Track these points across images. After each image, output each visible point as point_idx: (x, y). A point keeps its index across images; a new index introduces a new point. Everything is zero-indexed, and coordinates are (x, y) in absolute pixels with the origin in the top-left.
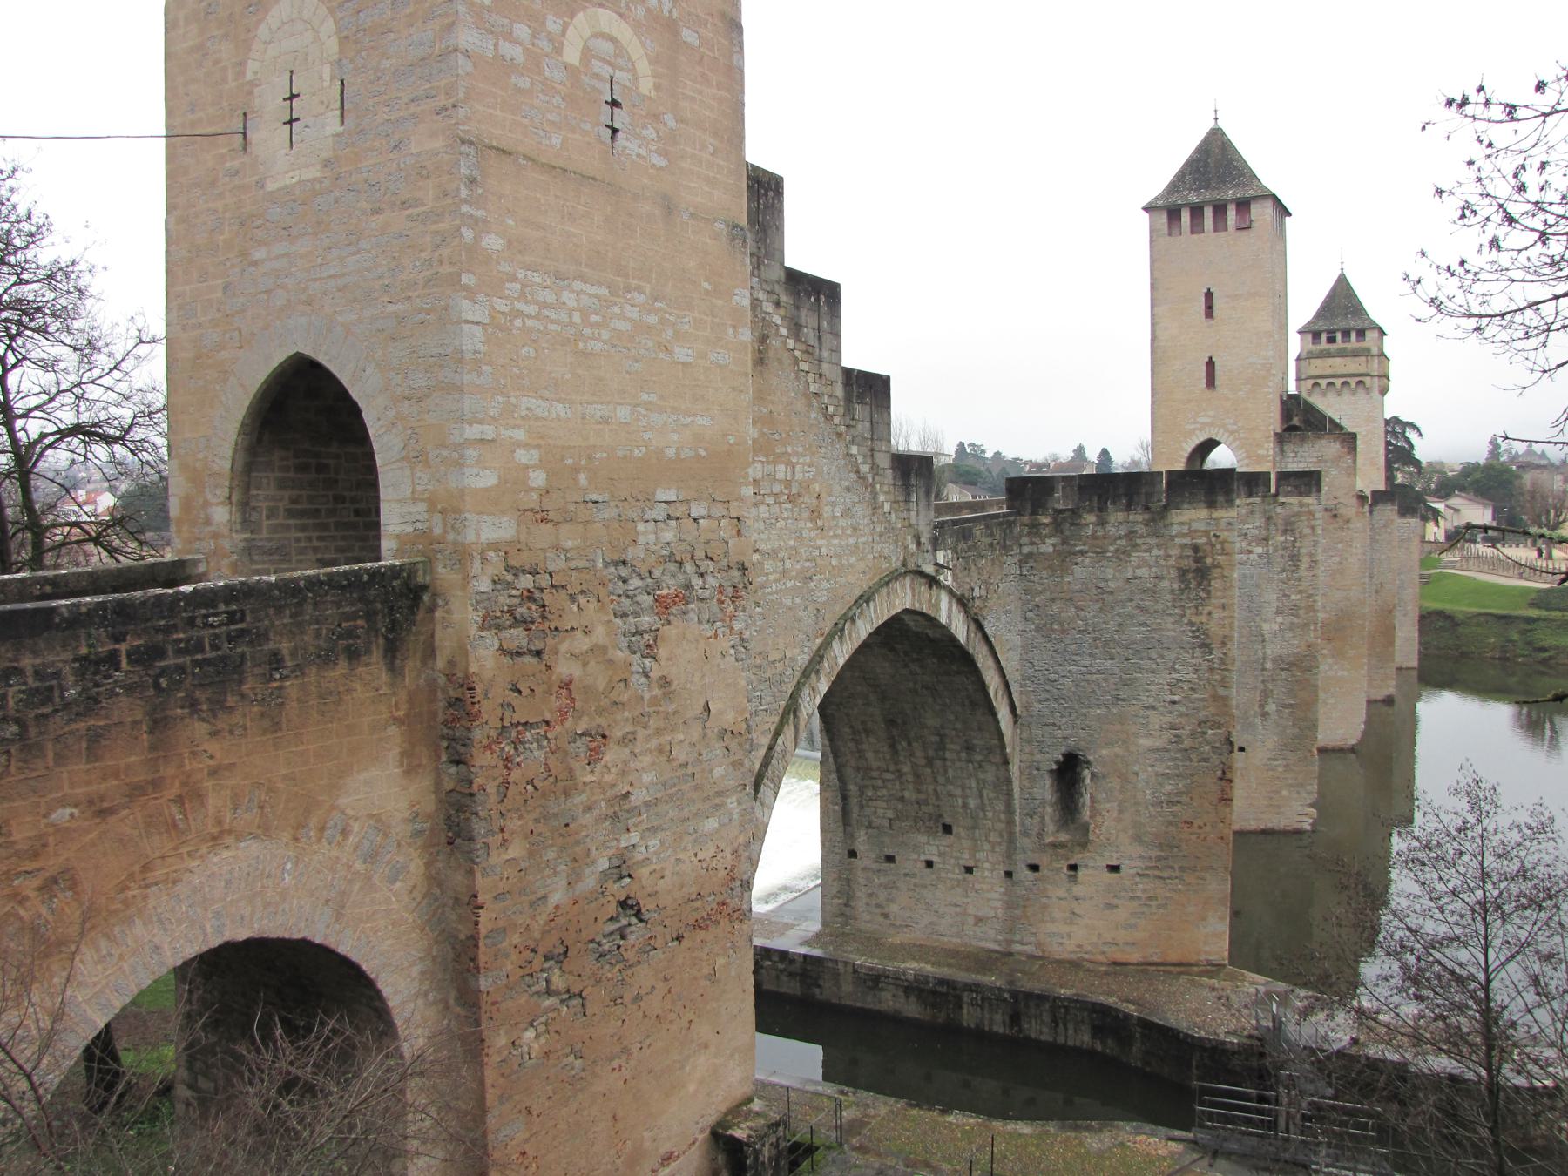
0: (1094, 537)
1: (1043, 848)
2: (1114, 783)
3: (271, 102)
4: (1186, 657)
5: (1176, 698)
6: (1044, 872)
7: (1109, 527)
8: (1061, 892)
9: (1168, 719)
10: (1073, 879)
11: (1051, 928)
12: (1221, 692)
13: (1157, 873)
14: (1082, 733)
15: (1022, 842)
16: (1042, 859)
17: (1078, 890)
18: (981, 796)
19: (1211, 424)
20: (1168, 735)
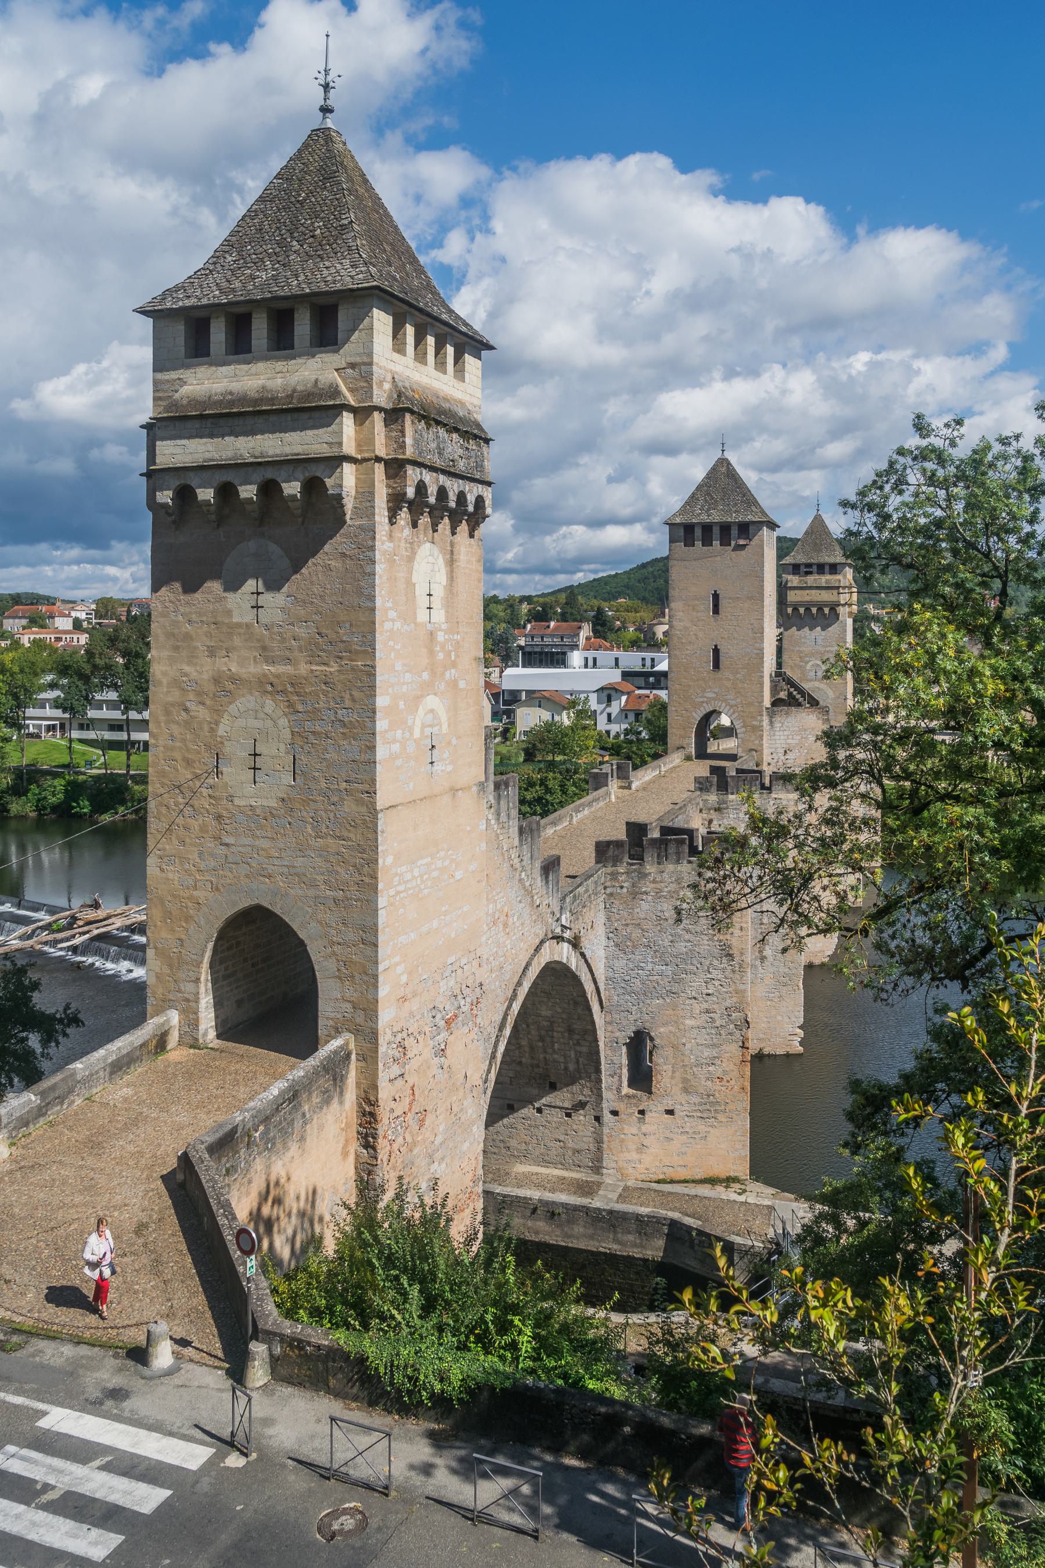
1: (621, 1098)
2: (669, 1052)
4: (716, 962)
6: (622, 1116)
7: (665, 875)
8: (634, 1131)
9: (705, 1006)
10: (642, 1121)
11: (627, 1156)
12: (742, 987)
14: (647, 1017)
15: (606, 1094)
16: (620, 1107)
17: (644, 1128)
18: (578, 1062)
20: (705, 1017)
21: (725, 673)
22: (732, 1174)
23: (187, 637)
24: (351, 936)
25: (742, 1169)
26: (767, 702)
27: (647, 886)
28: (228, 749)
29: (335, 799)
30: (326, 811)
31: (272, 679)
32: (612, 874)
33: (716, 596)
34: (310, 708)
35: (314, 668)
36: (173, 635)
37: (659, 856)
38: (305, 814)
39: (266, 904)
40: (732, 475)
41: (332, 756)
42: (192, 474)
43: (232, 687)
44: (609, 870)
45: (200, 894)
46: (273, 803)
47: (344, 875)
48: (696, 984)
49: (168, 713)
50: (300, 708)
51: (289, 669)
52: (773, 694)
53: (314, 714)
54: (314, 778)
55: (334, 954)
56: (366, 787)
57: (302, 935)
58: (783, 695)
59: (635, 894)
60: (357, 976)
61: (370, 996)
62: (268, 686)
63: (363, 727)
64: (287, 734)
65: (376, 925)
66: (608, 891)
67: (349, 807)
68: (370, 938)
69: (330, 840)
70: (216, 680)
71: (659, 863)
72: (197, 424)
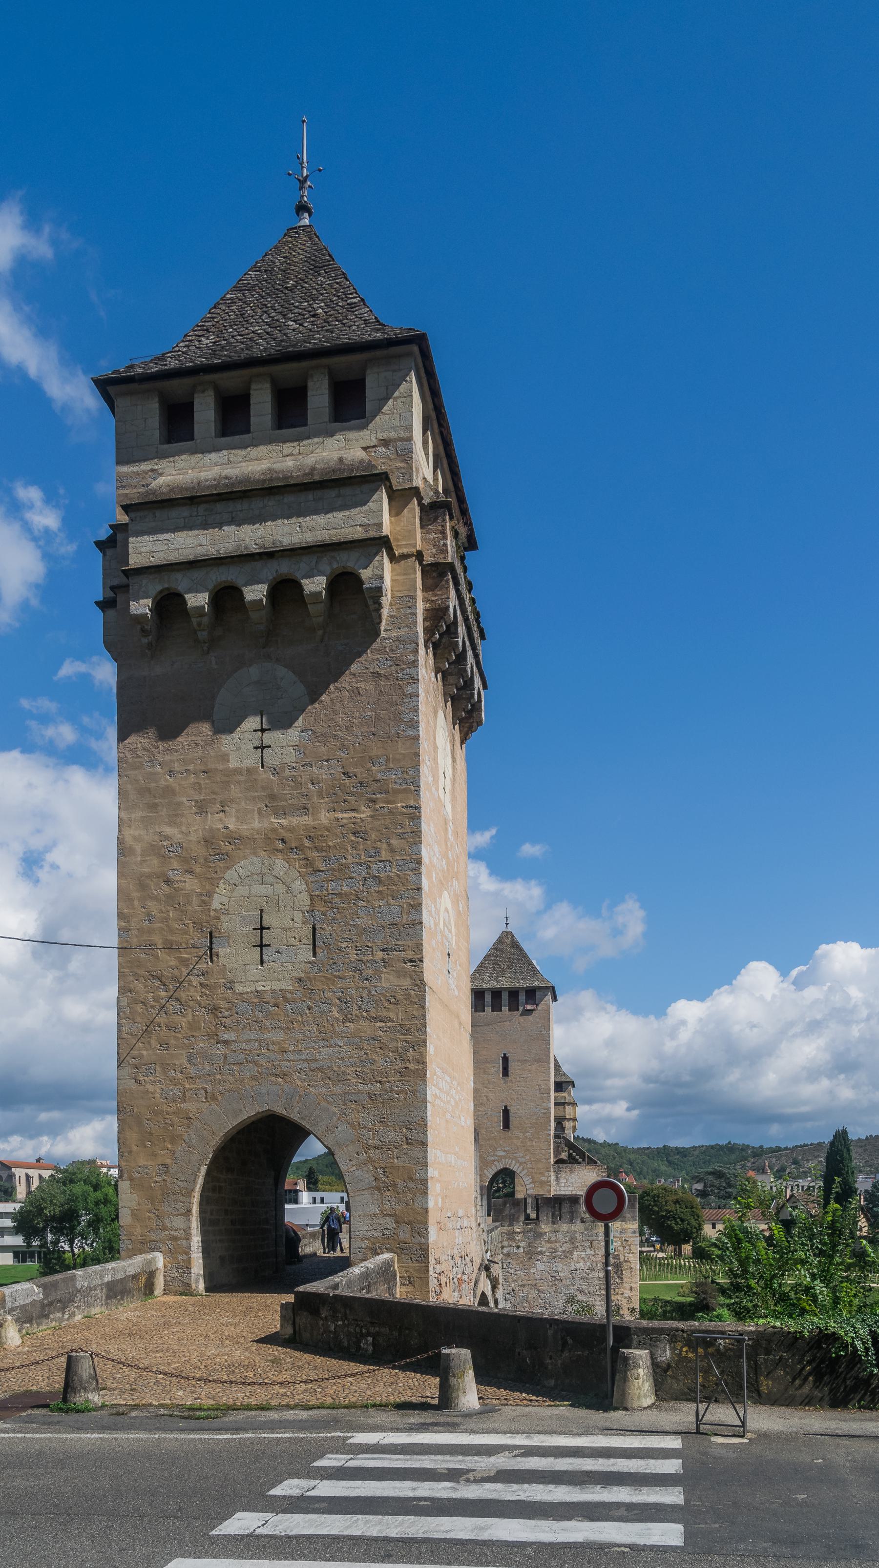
3: (237, 927)
19: (505, 1157)
21: (514, 1132)
26: (552, 1161)
29: (369, 972)
30: (357, 988)
33: (505, 1059)
34: (335, 865)
40: (516, 946)
41: (364, 920)
44: (506, 1229)
47: (381, 1062)
50: (321, 866)
51: (307, 820)
52: (555, 1156)
54: (340, 950)
55: (370, 1160)
56: (410, 954)
62: (279, 844)
64: (304, 900)
67: (388, 980)
69: (363, 1024)
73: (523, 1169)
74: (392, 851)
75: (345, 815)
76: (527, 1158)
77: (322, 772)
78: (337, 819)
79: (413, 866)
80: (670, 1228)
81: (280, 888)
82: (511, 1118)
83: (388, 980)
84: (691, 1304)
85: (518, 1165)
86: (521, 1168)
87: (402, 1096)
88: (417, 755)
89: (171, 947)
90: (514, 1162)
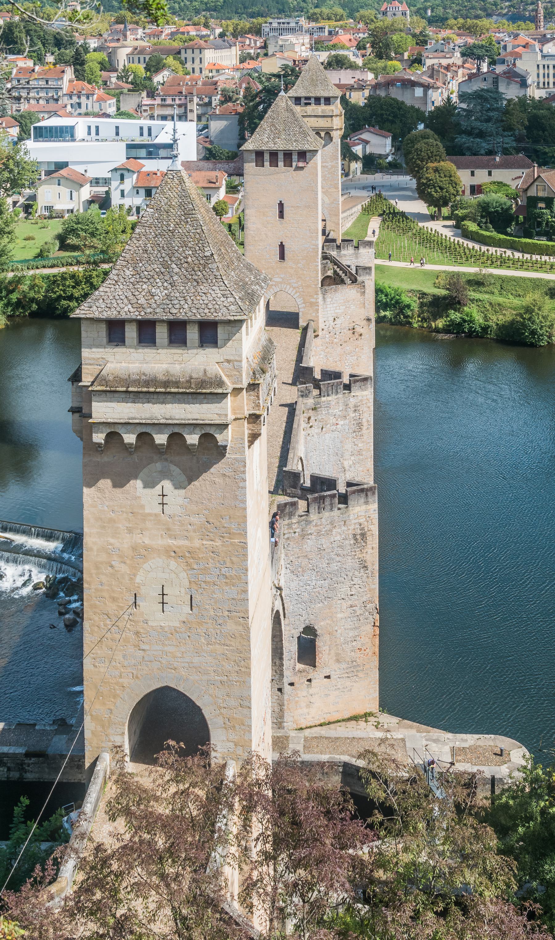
0: (316, 525)
2: (327, 637)
4: (356, 573)
5: (353, 593)
7: (323, 520)
13: (347, 675)
15: (286, 673)
20: (350, 610)
22: (368, 711)
23: (111, 520)
24: (233, 702)
25: (373, 706)
27: (311, 529)
28: (143, 591)
29: (220, 621)
30: (214, 629)
31: (175, 549)
32: (288, 525)
34: (202, 567)
35: (204, 542)
36: (101, 519)
37: (319, 508)
38: (199, 630)
39: (172, 685)
41: (218, 595)
42: (120, 426)
43: (145, 553)
45: (125, 681)
46: (177, 624)
47: (227, 666)
48: (344, 589)
49: (97, 568)
50: (195, 567)
51: (186, 543)
52: (323, 274)
53: (205, 571)
54: (206, 609)
56: (243, 615)
57: (198, 703)
58: (330, 273)
59: (304, 536)
60: (237, 727)
61: (246, 738)
63: (239, 578)
65: (250, 696)
66: (286, 536)
67: (231, 627)
68: (246, 703)
69: (217, 646)
70: (134, 548)
71: (319, 513)
72: (123, 396)
73: (296, 292)
74: (233, 563)
75: (208, 543)
76: (300, 283)
77: (194, 519)
78: (203, 544)
79: (244, 571)
80: (430, 194)
81: (173, 576)
82: (286, 252)
83: (231, 627)
84: (445, 298)
85: (292, 289)
86: (294, 291)
87: (238, 684)
88: (246, 517)
89: (114, 599)
90: (288, 287)
